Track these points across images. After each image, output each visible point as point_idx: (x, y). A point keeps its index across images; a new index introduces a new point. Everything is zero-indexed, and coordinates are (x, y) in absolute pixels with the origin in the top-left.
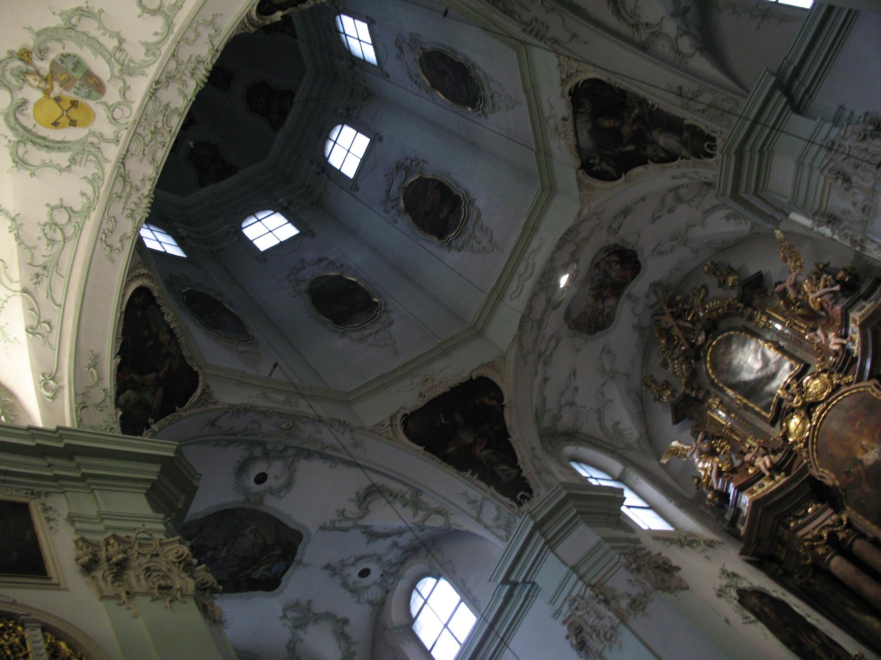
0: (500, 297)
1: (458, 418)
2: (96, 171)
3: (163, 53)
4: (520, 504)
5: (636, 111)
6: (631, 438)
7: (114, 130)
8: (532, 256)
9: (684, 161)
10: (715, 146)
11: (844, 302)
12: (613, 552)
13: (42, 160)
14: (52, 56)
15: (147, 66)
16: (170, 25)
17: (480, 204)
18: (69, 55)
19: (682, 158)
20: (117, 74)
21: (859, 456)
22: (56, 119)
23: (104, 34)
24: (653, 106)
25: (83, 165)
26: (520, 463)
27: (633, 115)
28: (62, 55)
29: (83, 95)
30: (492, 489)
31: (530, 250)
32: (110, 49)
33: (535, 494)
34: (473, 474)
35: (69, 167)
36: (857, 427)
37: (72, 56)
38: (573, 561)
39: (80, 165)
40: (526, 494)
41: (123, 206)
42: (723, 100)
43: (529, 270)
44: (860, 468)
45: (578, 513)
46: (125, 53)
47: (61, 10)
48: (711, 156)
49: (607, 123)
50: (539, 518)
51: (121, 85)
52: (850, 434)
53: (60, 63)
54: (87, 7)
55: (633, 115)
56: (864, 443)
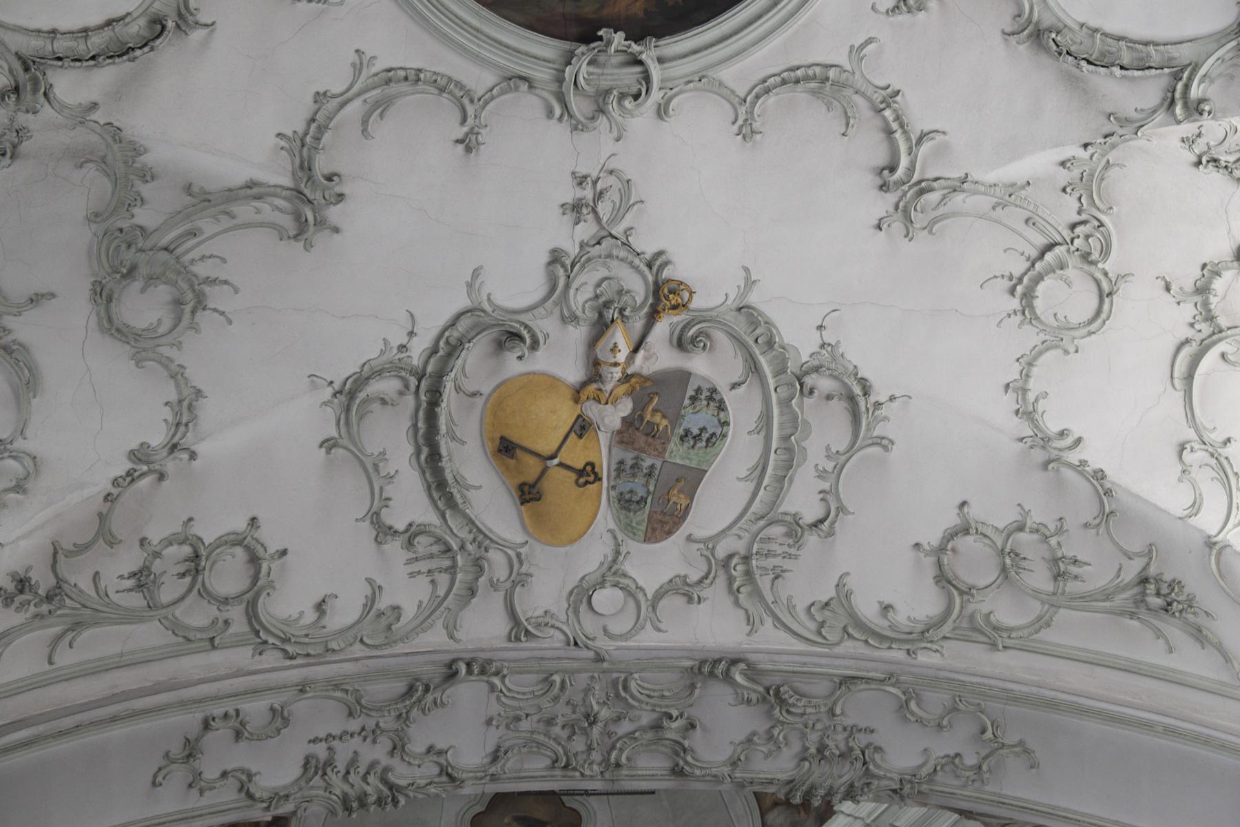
2: (409, 611)
3: (838, 650)
7: (554, 610)
13: (383, 453)
14: (699, 365)
15: (779, 623)
16: (924, 634)
18: (721, 407)
20: (721, 552)
22: (526, 444)
23: (822, 474)
25: (415, 567)
28: (714, 390)
29: (624, 486)
32: (790, 505)
35: (392, 532)
37: (722, 415)
39: (409, 562)
41: (336, 731)
46: (793, 551)
47: (838, 342)
51: (694, 577)
53: (690, 392)
54: (878, 405)
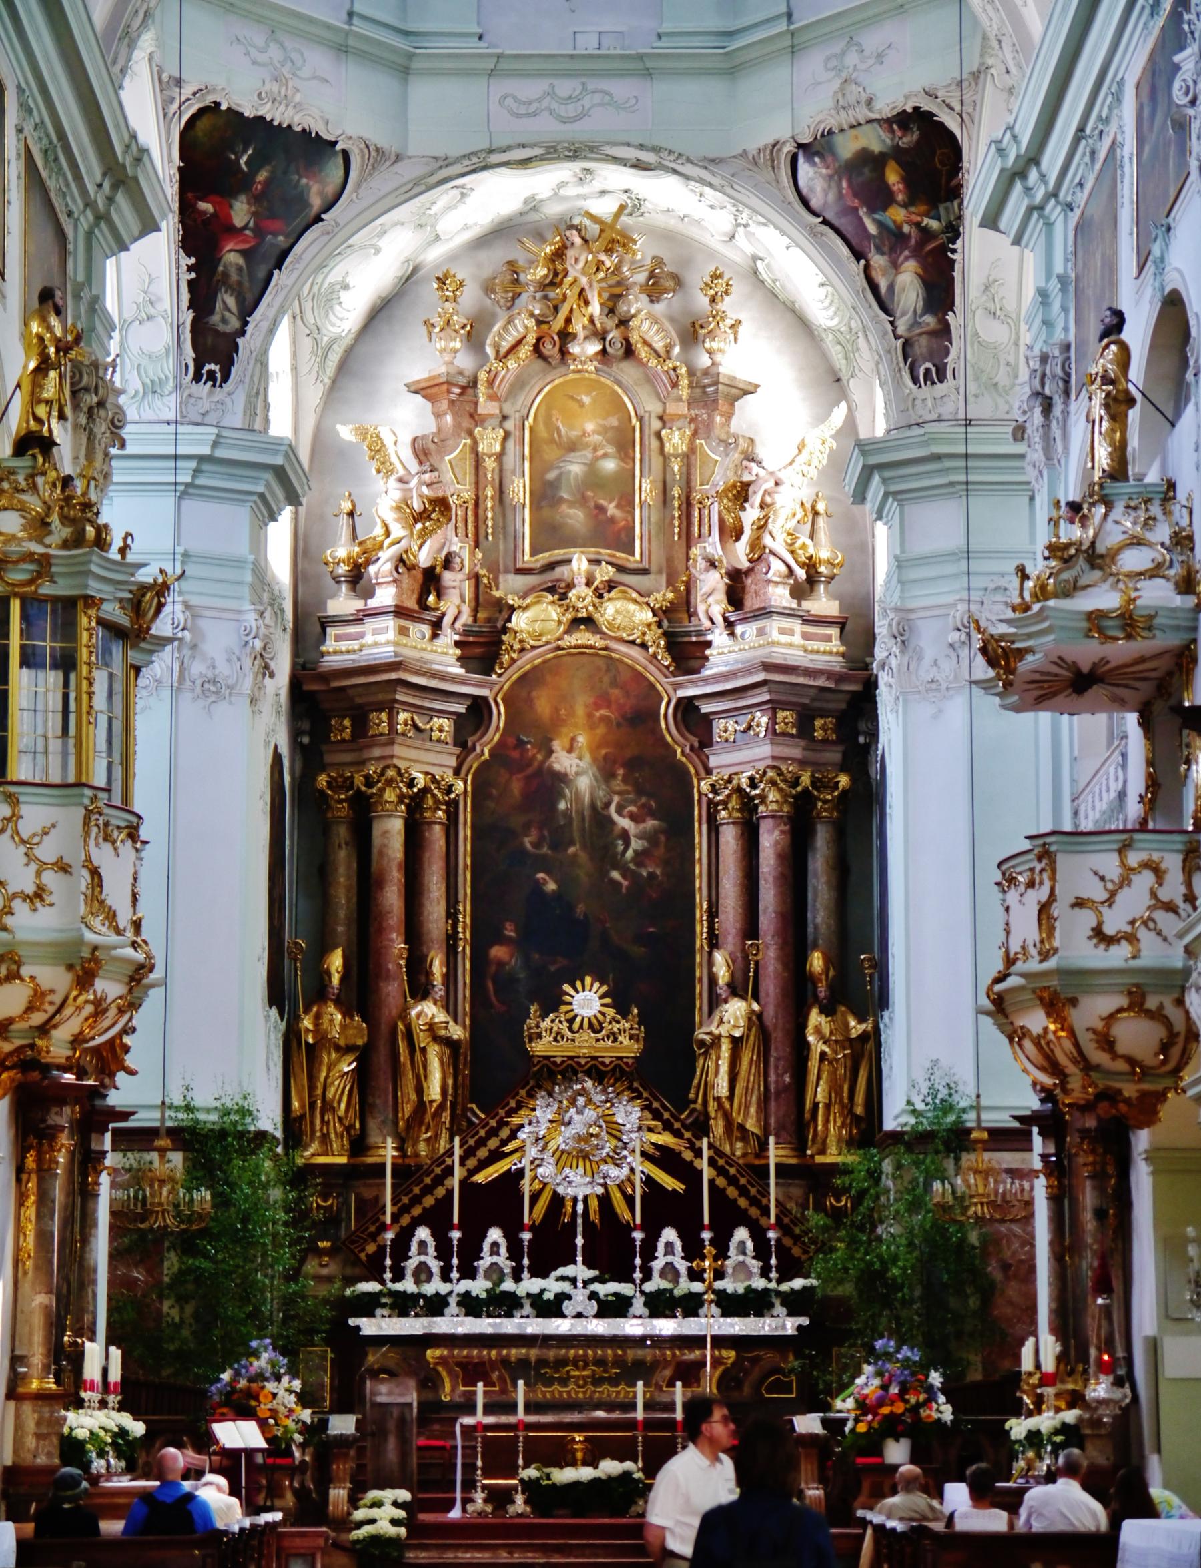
0: (491, 73)
1: (262, 176)
4: (197, 378)
5: (934, 224)
6: (333, 325)
8: (597, 98)
9: (889, 327)
10: (933, 383)
11: (780, 596)
12: (246, 591)
19: (892, 323)
21: (556, 745)
24: (954, 251)
26: (253, 320)
27: (926, 221)
30: (189, 316)
31: (605, 85)
33: (228, 386)
34: (190, 269)
36: (598, 714)
38: (190, 543)
40: (218, 375)
42: (1008, 364)
43: (571, 110)
44: (540, 757)
45: (262, 496)
48: (915, 380)
50: (220, 453)
52: (580, 711)
55: (926, 221)
56: (581, 739)
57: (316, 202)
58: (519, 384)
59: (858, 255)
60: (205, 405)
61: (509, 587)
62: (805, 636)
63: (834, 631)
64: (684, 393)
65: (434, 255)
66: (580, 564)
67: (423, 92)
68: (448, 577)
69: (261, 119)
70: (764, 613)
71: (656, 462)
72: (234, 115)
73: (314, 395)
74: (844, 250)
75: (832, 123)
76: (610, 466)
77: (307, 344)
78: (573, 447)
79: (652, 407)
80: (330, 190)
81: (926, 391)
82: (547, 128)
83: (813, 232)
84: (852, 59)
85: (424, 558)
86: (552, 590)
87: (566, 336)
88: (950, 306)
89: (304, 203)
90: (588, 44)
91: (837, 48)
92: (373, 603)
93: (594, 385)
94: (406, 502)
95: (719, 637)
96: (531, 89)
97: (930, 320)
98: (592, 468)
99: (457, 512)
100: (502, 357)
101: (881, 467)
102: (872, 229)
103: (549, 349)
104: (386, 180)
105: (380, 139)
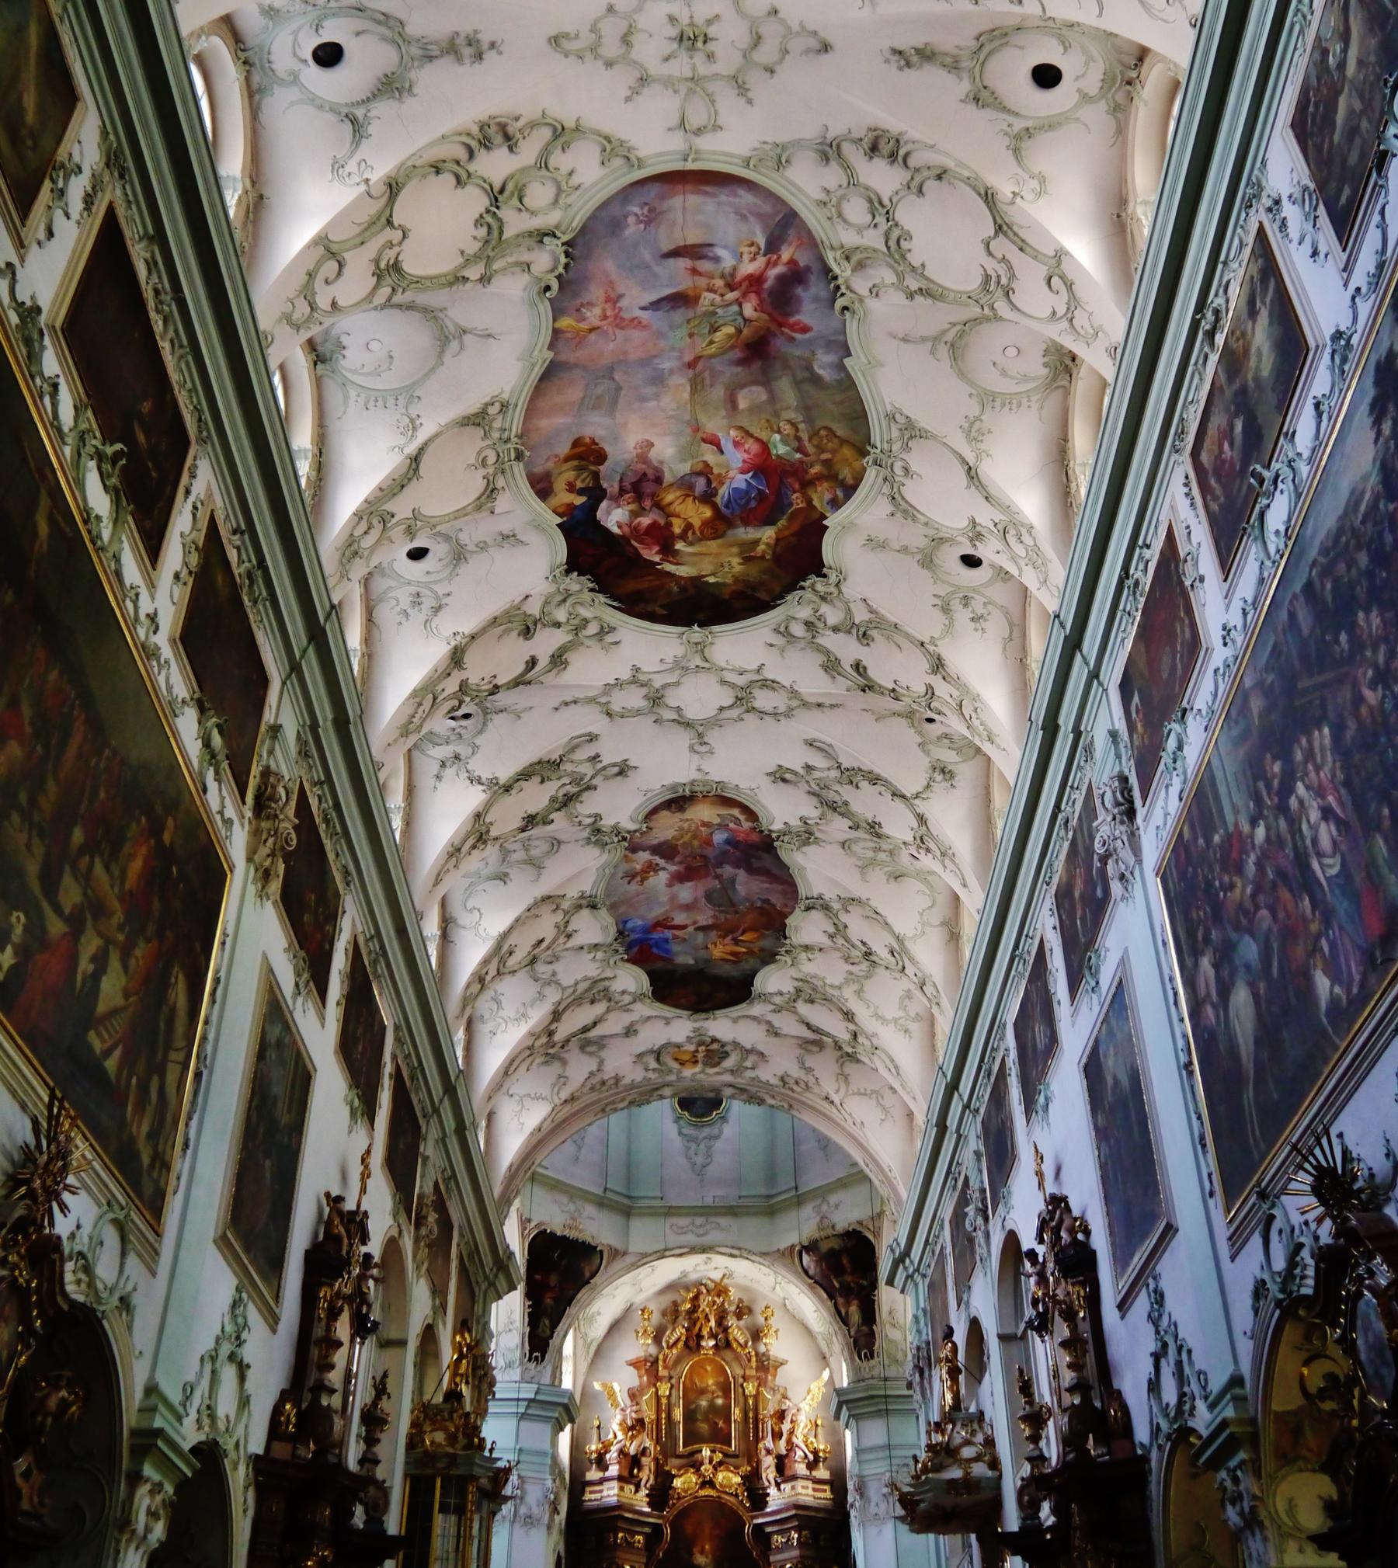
4: (530, 1360)
11: (801, 1469)
17: (728, 1130)
30: (528, 1330)
49: (845, 1261)
50: (540, 1397)
57: (587, 1274)
58: (678, 1361)
59: (831, 1297)
60: (532, 1373)
61: (672, 1466)
62: (814, 1490)
63: (827, 1487)
64: (754, 1364)
65: (639, 1299)
66: (706, 1452)
67: (637, 1225)
68: (645, 1460)
69: (564, 1237)
70: (794, 1478)
71: (741, 1400)
72: (552, 1234)
73: (583, 1367)
74: (825, 1295)
75: (817, 1236)
76: (720, 1401)
77: (581, 1342)
78: (703, 1392)
79: (739, 1372)
80: (594, 1268)
81: (865, 1364)
82: (690, 1239)
83: (811, 1288)
84: (824, 1207)
85: (632, 1451)
86: (693, 1466)
87: (700, 1337)
88: (874, 1321)
89: (583, 1274)
90: (709, 1201)
91: (818, 1202)
92: (608, 1474)
93: (712, 1361)
94: (624, 1421)
95: (772, 1491)
96: (683, 1222)
97: (865, 1329)
98: (712, 1403)
99: (648, 1426)
100: (670, 1347)
101: (847, 1402)
102: (837, 1285)
103: (692, 1343)
104: (618, 1265)
105: (617, 1244)
